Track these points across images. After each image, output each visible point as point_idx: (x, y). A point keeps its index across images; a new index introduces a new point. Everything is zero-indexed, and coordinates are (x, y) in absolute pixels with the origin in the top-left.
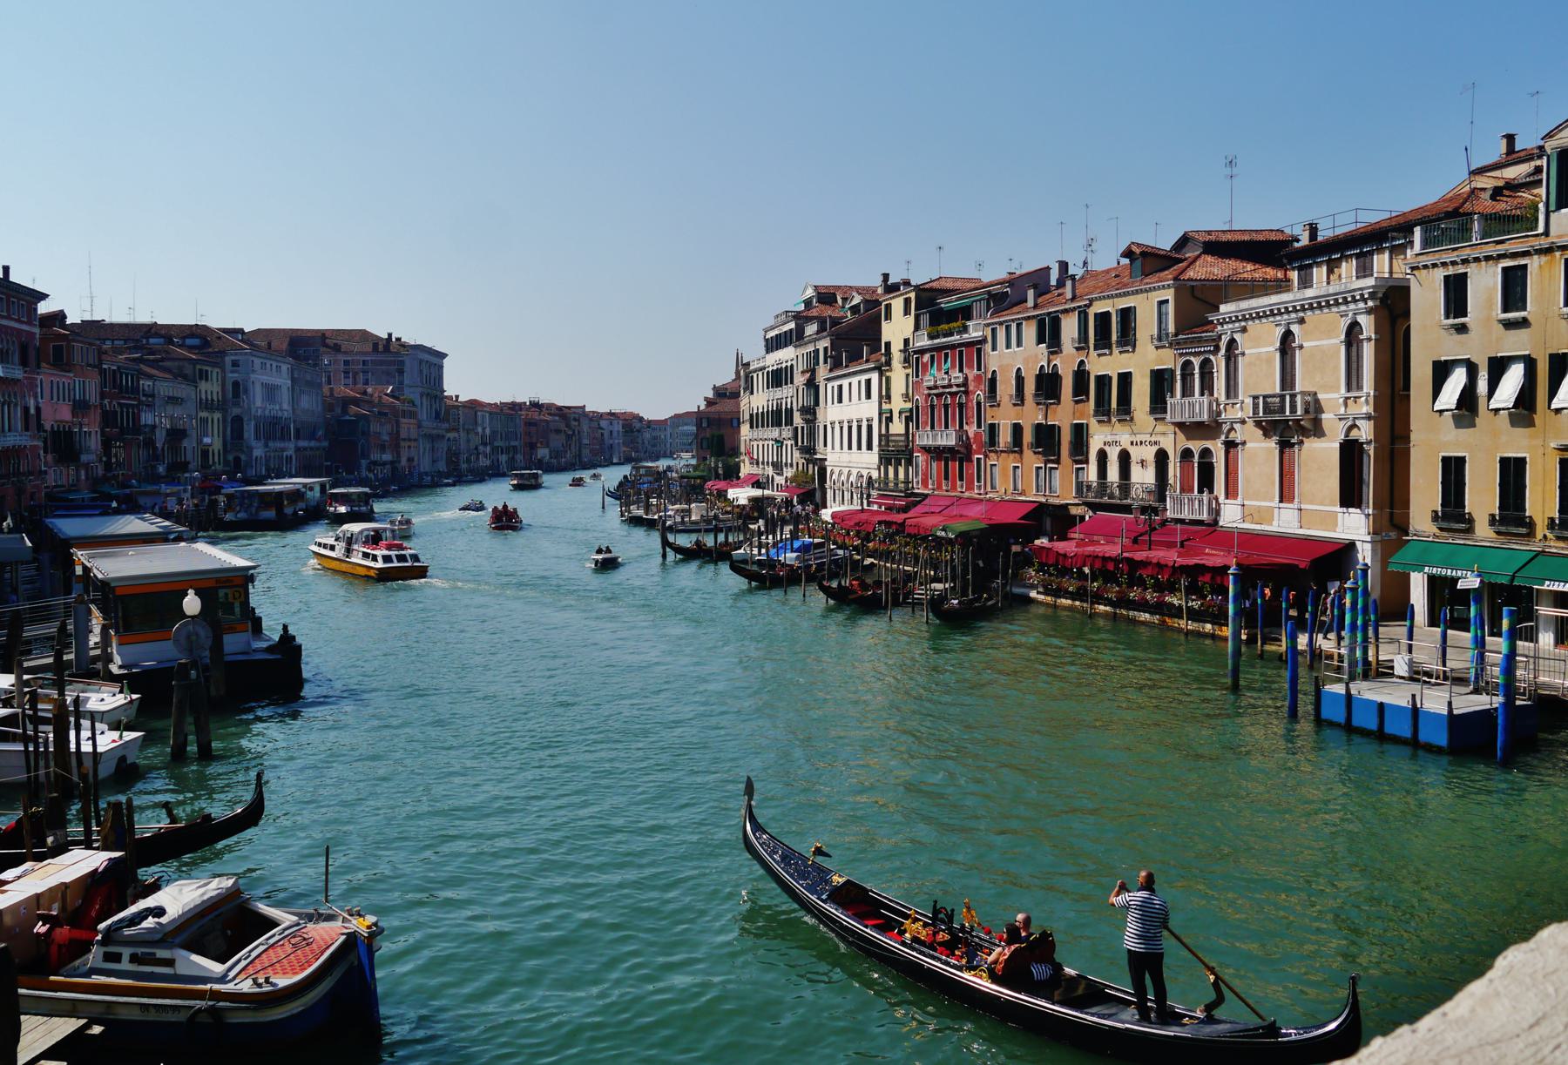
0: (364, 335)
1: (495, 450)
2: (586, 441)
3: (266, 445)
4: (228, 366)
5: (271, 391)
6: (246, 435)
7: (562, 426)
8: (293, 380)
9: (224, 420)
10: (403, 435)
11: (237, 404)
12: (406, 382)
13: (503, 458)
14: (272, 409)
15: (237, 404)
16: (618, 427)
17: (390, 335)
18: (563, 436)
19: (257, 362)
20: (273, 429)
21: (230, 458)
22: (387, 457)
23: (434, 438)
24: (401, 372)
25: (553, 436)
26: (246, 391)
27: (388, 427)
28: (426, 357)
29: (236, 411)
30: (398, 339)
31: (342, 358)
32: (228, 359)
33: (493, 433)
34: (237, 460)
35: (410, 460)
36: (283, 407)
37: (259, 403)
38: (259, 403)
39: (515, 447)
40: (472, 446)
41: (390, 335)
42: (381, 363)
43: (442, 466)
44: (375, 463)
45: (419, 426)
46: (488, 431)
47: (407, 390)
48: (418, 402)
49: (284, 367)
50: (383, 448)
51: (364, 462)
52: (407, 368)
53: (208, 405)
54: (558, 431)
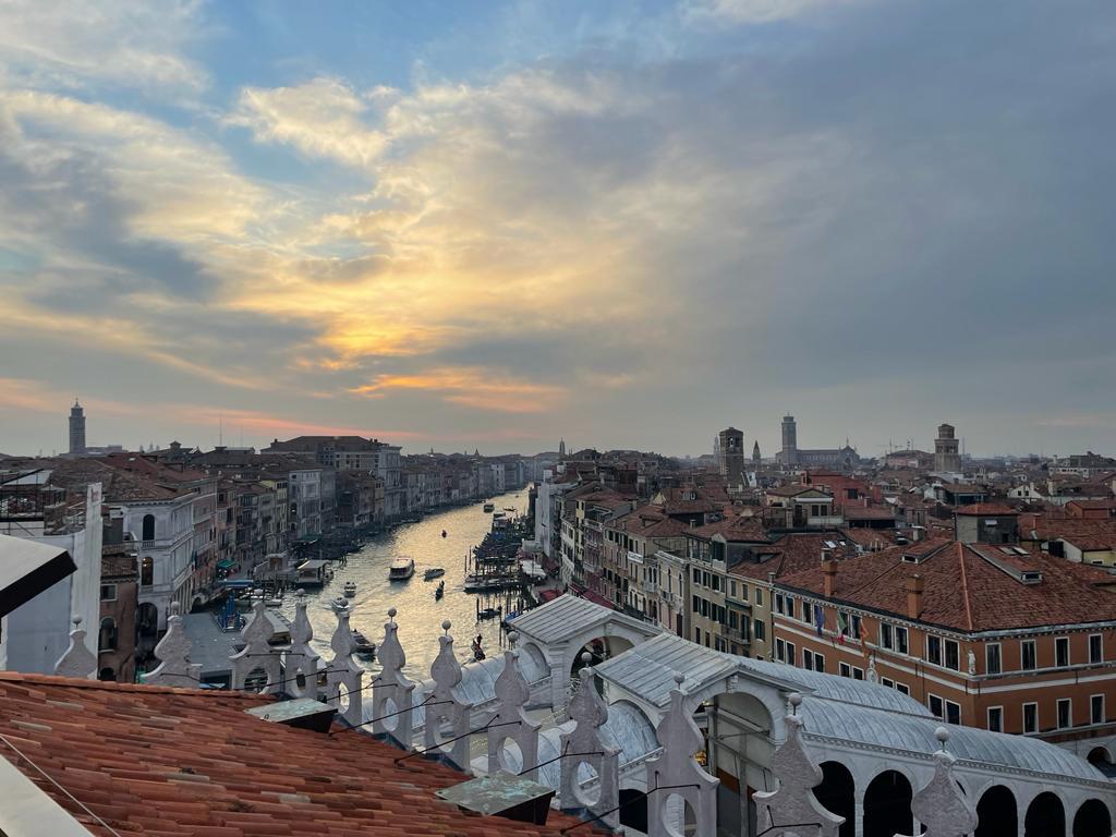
2: (482, 481)
5: (310, 487)
8: (321, 478)
10: (377, 497)
20: (310, 506)
21: (290, 524)
24: (377, 461)
25: (461, 482)
27: (369, 495)
29: (294, 501)
31: (346, 453)
32: (291, 475)
33: (427, 485)
34: (293, 525)
36: (315, 494)
50: (365, 506)
53: (281, 502)
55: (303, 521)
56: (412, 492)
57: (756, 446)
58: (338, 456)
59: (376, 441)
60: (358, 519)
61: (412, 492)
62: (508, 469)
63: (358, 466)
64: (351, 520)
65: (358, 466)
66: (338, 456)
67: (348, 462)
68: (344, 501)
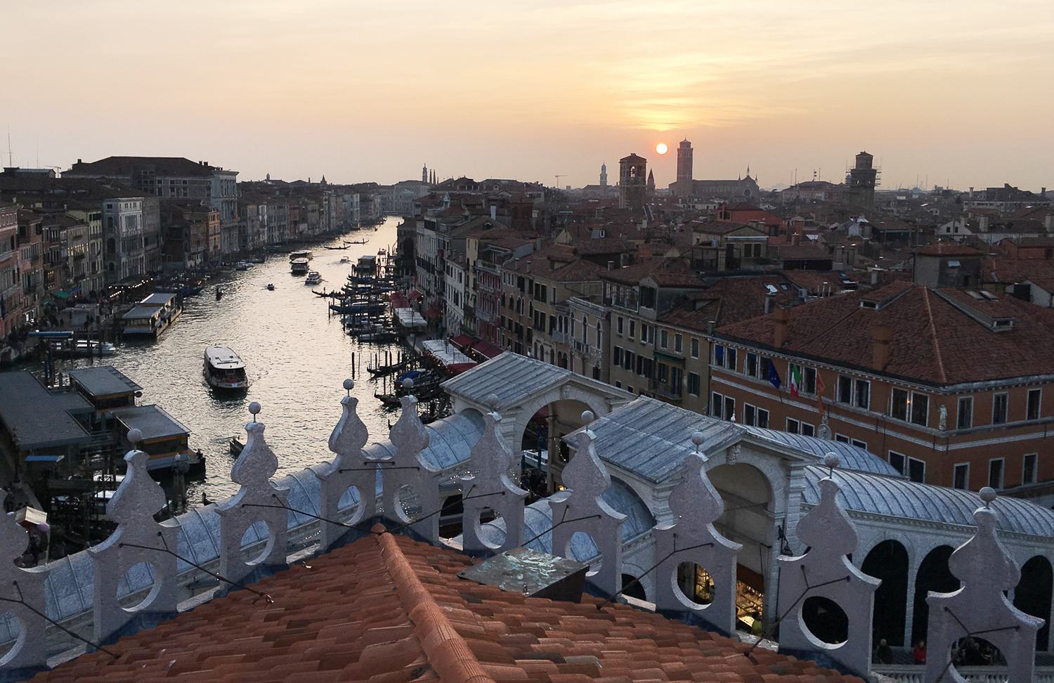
0: (182, 163)
1: (270, 229)
2: (333, 214)
3: (129, 255)
4: (105, 208)
5: (131, 220)
6: (117, 251)
7: (317, 206)
8: (143, 209)
9: (103, 240)
11: (111, 232)
12: (212, 195)
13: (276, 234)
14: (132, 232)
15: (111, 232)
16: (357, 198)
17: (201, 162)
18: (316, 214)
19: (123, 204)
20: (132, 243)
21: (108, 264)
22: (201, 249)
23: (229, 229)
24: (209, 188)
25: (309, 215)
26: (117, 223)
28: (225, 177)
29: (110, 236)
30: (206, 163)
31: (169, 179)
32: (105, 204)
34: (112, 265)
35: (215, 247)
37: (124, 230)
38: (124, 230)
39: (284, 226)
40: (255, 230)
41: (201, 162)
42: (195, 182)
43: (236, 249)
44: (194, 254)
45: (221, 223)
46: (266, 217)
47: (213, 201)
48: (220, 209)
49: (138, 203)
50: (198, 243)
51: (186, 254)
52: (213, 185)
54: (313, 211)
55: (124, 260)
56: (253, 227)
57: (604, 168)
58: (160, 182)
59: (206, 163)
60: (190, 259)
61: (253, 227)
62: (365, 200)
63: (185, 194)
64: (181, 259)
65: (185, 194)
66: (160, 182)
67: (172, 190)
68: (173, 236)
